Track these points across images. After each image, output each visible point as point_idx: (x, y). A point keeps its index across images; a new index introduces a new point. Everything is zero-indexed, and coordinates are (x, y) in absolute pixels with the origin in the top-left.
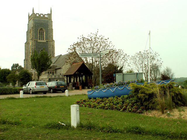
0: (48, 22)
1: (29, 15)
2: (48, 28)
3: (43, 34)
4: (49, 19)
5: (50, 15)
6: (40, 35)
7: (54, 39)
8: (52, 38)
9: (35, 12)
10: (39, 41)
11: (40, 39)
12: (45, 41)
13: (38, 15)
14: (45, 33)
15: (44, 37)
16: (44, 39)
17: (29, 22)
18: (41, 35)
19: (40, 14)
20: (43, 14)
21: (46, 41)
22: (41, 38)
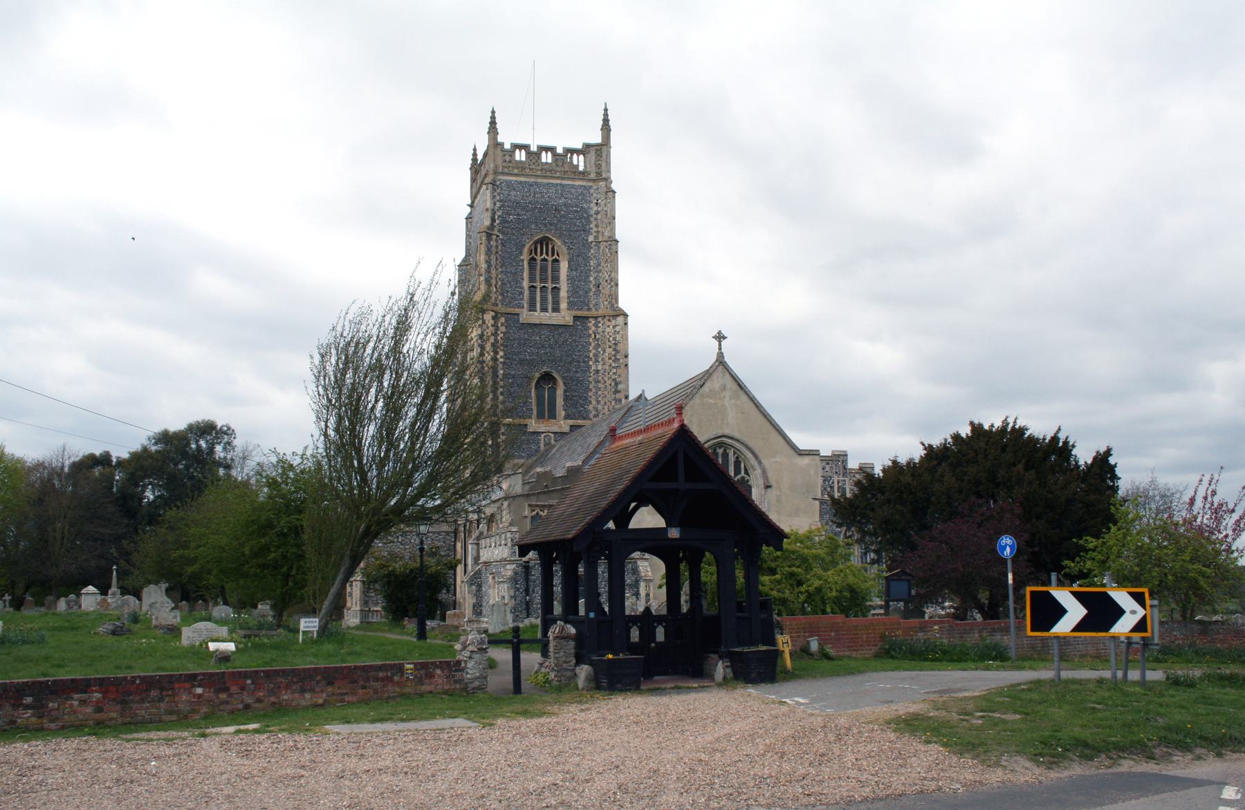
0: (584, 193)
1: (475, 155)
2: (588, 232)
3: (556, 270)
4: (593, 176)
5: (599, 152)
6: (532, 279)
7: (623, 304)
8: (614, 297)
9: (507, 138)
10: (526, 316)
11: (532, 307)
12: (565, 316)
13: (520, 156)
14: (564, 266)
15: (563, 293)
16: (563, 305)
17: (471, 206)
18: (544, 280)
19: (534, 148)
20: (552, 149)
21: (576, 318)
22: (544, 299)
